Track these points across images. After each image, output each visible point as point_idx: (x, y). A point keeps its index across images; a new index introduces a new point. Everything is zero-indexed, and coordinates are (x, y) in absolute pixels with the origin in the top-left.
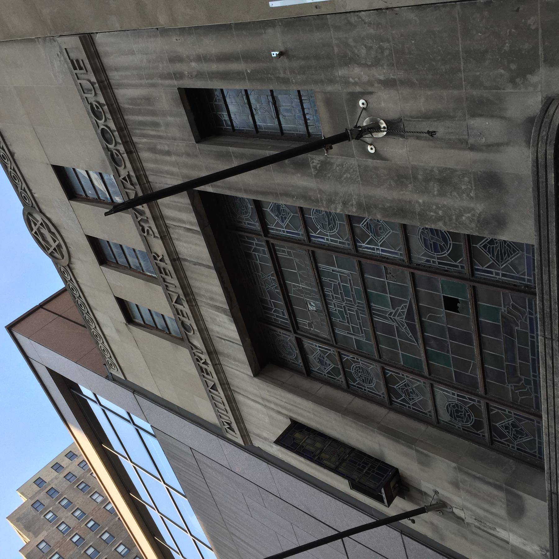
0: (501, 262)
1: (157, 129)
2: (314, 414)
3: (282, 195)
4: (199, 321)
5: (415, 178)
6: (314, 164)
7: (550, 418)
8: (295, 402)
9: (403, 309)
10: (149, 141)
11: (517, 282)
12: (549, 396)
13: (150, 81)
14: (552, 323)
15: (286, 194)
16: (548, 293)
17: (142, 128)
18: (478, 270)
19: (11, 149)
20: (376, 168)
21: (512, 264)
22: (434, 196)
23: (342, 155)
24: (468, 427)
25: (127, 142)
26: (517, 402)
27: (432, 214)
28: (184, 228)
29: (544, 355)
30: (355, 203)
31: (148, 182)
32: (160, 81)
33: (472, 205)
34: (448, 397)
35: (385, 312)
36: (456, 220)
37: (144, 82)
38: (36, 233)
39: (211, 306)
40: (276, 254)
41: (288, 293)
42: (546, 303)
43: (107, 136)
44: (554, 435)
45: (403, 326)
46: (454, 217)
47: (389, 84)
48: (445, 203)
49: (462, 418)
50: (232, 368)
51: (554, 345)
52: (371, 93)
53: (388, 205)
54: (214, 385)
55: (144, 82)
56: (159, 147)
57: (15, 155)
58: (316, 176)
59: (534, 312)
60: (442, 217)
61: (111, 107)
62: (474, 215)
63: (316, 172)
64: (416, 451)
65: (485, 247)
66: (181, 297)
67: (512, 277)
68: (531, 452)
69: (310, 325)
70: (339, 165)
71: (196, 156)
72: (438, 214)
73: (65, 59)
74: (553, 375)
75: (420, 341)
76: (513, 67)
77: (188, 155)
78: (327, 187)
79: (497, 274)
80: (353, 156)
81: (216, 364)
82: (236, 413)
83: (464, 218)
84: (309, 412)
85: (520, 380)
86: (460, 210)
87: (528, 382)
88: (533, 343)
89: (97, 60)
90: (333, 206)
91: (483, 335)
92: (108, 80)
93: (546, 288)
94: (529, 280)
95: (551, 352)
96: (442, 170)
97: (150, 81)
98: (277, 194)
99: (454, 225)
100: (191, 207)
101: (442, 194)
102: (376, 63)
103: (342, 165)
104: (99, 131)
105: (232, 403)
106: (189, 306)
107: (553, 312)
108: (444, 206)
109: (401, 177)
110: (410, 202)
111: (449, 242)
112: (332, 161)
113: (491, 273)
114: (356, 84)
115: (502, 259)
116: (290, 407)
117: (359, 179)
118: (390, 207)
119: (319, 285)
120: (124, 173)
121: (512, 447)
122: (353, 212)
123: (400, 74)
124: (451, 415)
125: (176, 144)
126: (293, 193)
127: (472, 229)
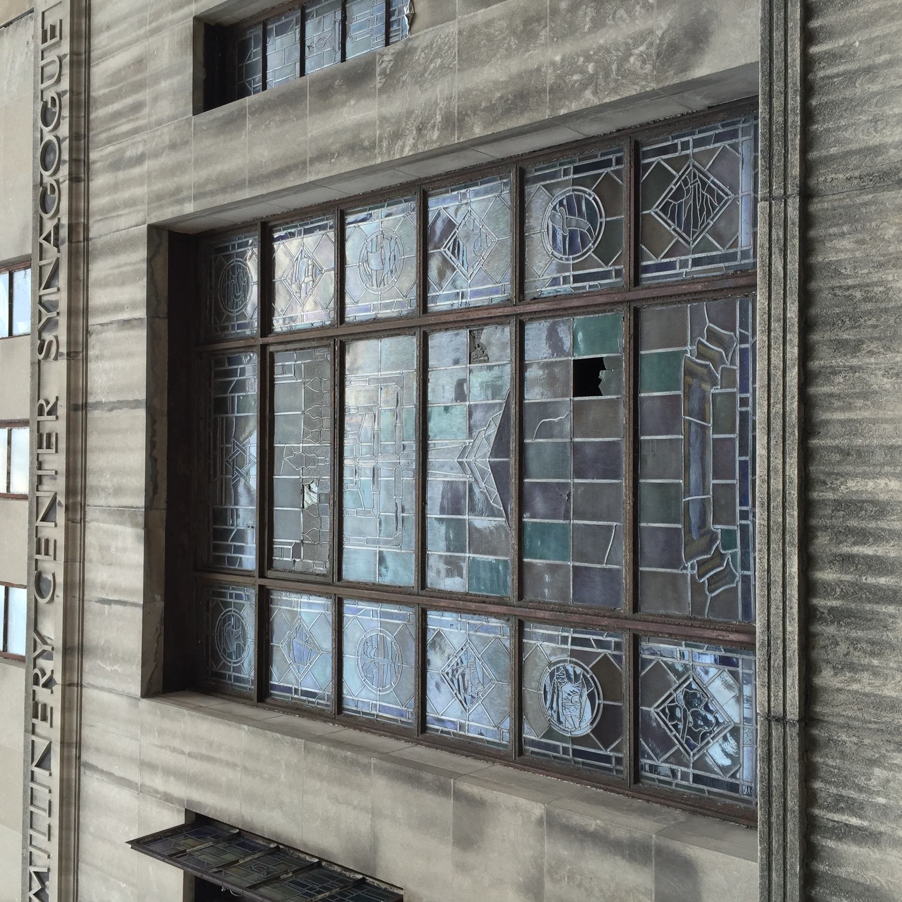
0: (694, 233)
1: (137, 116)
2: (245, 769)
3: (313, 161)
4: (74, 561)
5: (555, 11)
6: (384, 65)
7: (773, 443)
8: (210, 744)
10: (118, 146)
11: (720, 269)
12: (773, 372)
13: (154, 25)
14: (786, 151)
15: (322, 156)
16: (782, 75)
17: (111, 125)
18: (647, 269)
20: (489, 23)
22: (584, 35)
23: (434, 24)
25: (78, 161)
26: (702, 613)
27: (575, 77)
28: (118, 322)
29: (766, 252)
30: (439, 118)
31: (87, 239)
32: (171, 16)
33: (650, 23)
36: (618, 69)
37: (142, 31)
39: (110, 513)
40: (272, 380)
41: (272, 473)
42: (777, 104)
43: (50, 157)
44: (780, 499)
46: (614, 67)
48: (602, 41)
50: (102, 689)
51: (790, 209)
53: (498, 95)
54: (48, 751)
55: (142, 31)
56: (128, 154)
58: (382, 91)
59: (750, 334)
60: (593, 75)
61: (75, 97)
62: (651, 44)
63: (384, 80)
64: (459, 796)
65: (664, 210)
67: (711, 260)
68: (727, 779)
70: (427, 47)
71: (186, 143)
72: (587, 72)
73: (35, 32)
74: (785, 303)
75: (513, 505)
77: (173, 147)
78: (394, 106)
79: (684, 264)
80: (452, 17)
81: (71, 685)
82: (68, 839)
83: (632, 59)
84: (234, 766)
85: (713, 540)
86: (627, 44)
87: (729, 542)
88: (744, 416)
89: (83, 21)
90: (400, 143)
91: (642, 438)
92: (89, 53)
93: (778, 62)
94: (745, 255)
95: (781, 236)
97: (154, 25)
98: (304, 163)
99: (612, 85)
100: (144, 266)
101: (598, 24)
103: (430, 46)
105: (69, 804)
106: (67, 520)
107: (790, 120)
108: (600, 48)
110: (538, 70)
111: (599, 220)
112: (416, 43)
115: (695, 226)
116: (195, 766)
117: (456, 62)
118: (501, 98)
119: (337, 426)
120: (49, 226)
121: (685, 776)
122: (433, 142)
125: (158, 133)
126: (333, 148)
127: (645, 78)
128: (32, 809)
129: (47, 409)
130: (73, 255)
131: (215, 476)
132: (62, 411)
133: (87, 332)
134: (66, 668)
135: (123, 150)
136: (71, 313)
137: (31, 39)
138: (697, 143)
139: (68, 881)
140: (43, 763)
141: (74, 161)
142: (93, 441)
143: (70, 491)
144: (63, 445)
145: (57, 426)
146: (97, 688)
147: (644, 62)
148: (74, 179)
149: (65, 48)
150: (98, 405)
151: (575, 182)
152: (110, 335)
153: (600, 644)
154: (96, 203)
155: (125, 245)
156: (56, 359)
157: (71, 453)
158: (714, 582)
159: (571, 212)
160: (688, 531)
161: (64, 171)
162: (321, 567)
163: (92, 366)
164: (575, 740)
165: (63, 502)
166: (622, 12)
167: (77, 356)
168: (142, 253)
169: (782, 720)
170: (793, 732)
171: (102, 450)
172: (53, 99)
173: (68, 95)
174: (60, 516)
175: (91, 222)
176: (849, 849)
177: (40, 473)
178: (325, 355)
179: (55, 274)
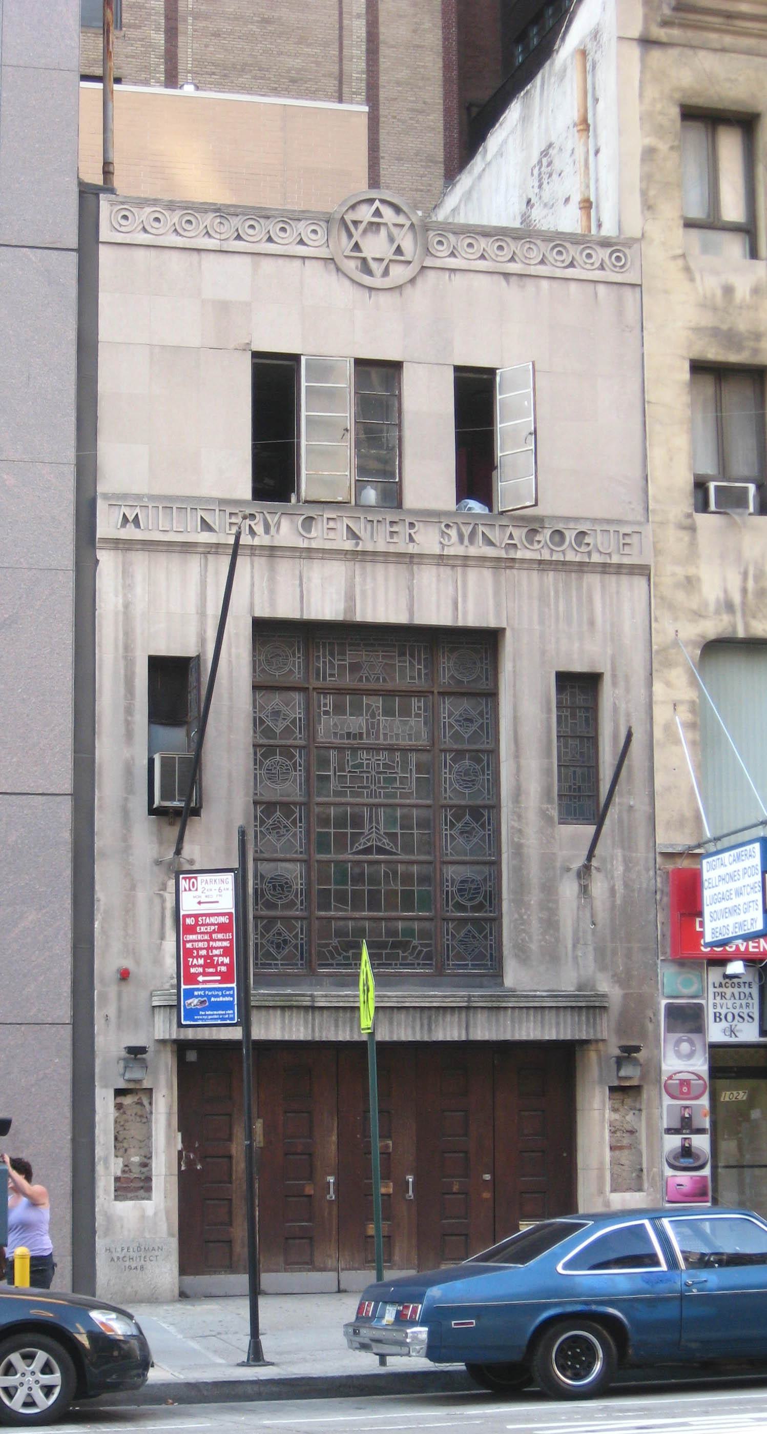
4: (323, 553)
9: (386, 843)
18: (448, 924)
19: (513, 279)
21: (459, 953)
24: (263, 895)
34: (296, 877)
35: (378, 823)
37: (608, 627)
38: (377, 213)
45: (368, 840)
47: (613, 891)
49: (274, 889)
50: (252, 577)
52: (606, 877)
57: (503, 283)
65: (469, 931)
66: (361, 542)
69: (326, 713)
76: (623, 976)
79: (448, 940)
88: (390, 964)
94: (448, 965)
96: (557, 922)
101: (541, 920)
102: (626, 885)
104: (560, 526)
109: (549, 889)
113: (448, 935)
114: (613, 865)
123: (618, 902)
124: (272, 878)
128: (174, 509)
129: (412, 531)
130: (498, 559)
131: (365, 645)
132: (411, 549)
133: (453, 566)
134: (262, 547)
135: (549, 606)
136: (466, 557)
137: (632, 506)
138: (491, 945)
139: (137, 544)
140: (206, 526)
141: (551, 562)
142: (392, 567)
143: (364, 553)
144: (392, 549)
145: (402, 546)
146: (252, 572)
147: (522, 940)
148: (540, 562)
149: (615, 559)
150: (412, 574)
151: (486, 891)
152: (451, 589)
153: (302, 901)
154: (525, 573)
155: (498, 615)
156: (441, 543)
157: (386, 554)
158: (330, 952)
159: (475, 889)
160: (349, 942)
161: (546, 556)
162: (322, 736)
163: (434, 569)
164: (262, 889)
165: (359, 549)
166: (542, 930)
167: (441, 560)
168: (492, 623)
169: (314, 1001)
170: (309, 1004)
171: (386, 579)
172: (588, 544)
173: (587, 560)
174: (349, 545)
175: (515, 571)
176: (279, 1021)
177: (375, 522)
178: (423, 742)
179: (490, 543)
